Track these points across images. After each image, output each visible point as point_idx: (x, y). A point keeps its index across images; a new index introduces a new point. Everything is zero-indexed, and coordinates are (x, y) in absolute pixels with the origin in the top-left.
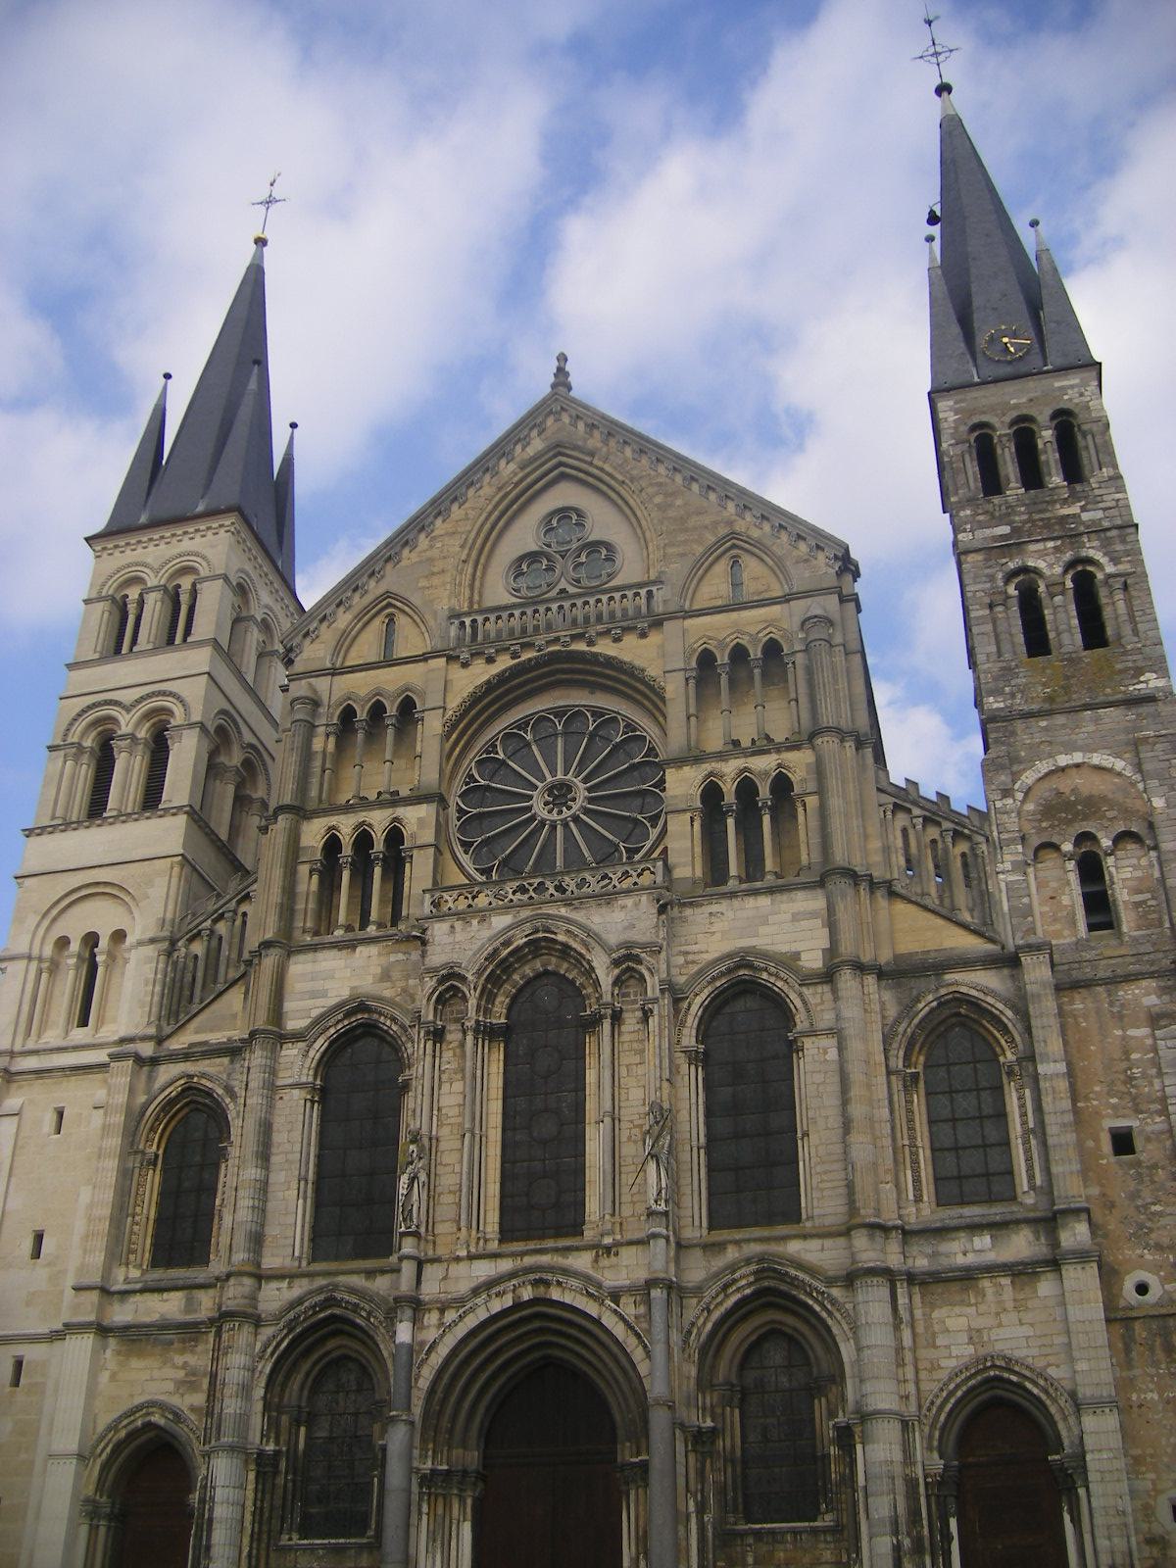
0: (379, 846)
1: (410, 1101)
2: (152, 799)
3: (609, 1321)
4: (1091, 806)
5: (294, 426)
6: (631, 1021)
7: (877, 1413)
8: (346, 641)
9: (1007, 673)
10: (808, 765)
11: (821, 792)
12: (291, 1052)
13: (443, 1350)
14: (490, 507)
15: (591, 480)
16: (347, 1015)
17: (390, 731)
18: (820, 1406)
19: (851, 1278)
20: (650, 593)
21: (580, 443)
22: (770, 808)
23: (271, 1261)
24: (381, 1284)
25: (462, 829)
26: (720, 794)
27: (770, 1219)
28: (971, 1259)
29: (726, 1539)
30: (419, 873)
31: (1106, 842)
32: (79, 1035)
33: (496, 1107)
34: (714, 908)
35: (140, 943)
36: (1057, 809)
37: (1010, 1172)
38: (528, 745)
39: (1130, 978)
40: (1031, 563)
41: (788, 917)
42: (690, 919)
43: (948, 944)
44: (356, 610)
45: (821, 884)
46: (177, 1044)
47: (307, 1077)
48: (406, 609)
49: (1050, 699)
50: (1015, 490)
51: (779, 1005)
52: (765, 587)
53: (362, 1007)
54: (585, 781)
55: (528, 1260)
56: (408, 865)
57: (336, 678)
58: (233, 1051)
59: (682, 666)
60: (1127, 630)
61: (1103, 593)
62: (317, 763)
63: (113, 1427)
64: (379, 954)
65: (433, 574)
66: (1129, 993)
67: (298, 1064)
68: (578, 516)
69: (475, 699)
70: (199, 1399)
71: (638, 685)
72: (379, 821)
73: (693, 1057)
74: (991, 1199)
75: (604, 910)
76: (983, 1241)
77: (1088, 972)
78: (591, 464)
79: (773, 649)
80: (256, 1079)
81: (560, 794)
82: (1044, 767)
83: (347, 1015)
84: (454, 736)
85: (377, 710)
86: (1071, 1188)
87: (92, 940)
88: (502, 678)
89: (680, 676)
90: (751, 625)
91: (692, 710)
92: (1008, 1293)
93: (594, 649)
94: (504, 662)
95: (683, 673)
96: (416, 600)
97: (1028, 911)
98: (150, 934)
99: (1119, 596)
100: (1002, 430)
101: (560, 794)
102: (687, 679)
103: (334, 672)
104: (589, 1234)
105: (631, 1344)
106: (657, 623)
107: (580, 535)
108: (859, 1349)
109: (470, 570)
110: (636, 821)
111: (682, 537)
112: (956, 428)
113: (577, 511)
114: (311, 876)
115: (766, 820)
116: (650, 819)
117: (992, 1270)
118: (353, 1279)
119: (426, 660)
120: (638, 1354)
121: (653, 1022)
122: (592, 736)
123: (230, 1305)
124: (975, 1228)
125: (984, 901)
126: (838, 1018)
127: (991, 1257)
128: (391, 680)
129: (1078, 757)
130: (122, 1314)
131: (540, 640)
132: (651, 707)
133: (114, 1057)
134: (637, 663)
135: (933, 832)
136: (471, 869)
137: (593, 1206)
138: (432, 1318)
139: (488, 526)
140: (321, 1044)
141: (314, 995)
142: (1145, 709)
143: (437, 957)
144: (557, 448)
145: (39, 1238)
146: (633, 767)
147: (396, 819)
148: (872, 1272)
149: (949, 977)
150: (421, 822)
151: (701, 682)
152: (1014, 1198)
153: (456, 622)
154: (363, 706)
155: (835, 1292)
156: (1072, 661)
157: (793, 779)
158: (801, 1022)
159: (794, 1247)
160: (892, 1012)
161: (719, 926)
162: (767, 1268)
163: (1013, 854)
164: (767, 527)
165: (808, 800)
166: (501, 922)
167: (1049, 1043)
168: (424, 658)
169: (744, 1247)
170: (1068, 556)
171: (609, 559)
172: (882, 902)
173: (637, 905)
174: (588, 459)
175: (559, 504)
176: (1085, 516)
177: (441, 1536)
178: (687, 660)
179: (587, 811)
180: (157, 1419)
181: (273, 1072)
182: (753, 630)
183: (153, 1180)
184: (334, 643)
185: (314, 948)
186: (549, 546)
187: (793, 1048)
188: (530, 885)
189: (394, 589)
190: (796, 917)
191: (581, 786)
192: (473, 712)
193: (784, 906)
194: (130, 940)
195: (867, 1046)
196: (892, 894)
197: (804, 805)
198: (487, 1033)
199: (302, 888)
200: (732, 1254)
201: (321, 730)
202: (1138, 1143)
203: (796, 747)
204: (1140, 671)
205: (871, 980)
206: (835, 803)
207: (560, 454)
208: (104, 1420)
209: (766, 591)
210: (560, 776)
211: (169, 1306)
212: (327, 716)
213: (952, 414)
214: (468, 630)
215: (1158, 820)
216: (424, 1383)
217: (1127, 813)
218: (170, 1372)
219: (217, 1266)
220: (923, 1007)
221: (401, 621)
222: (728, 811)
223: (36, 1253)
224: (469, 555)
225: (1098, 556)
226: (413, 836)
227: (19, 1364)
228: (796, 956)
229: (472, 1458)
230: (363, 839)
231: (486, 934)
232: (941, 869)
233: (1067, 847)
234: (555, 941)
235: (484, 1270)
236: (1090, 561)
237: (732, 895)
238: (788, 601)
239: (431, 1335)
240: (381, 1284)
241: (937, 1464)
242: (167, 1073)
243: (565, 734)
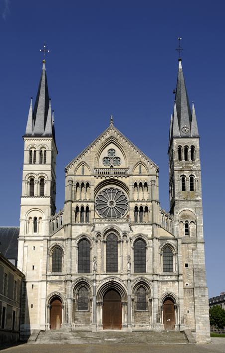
1: (92, 251)
2: (42, 194)
3: (122, 284)
4: (188, 216)
6: (125, 242)
7: (155, 298)
8: (76, 169)
9: (179, 193)
11: (152, 210)
12: (73, 241)
13: (100, 287)
16: (82, 236)
18: (147, 297)
19: (153, 281)
23: (73, 273)
24: (89, 277)
26: (137, 208)
27: (142, 272)
28: (167, 279)
29: (135, 312)
30: (91, 214)
31: (189, 222)
32: (35, 234)
33: (105, 253)
35: (45, 220)
36: (184, 216)
37: (173, 268)
39: (190, 243)
40: (185, 174)
43: (167, 235)
45: (152, 225)
46: (53, 237)
47: (76, 245)
49: (185, 198)
50: (184, 160)
51: (145, 242)
53: (84, 236)
55: (111, 275)
58: (63, 240)
60: (197, 189)
61: (194, 181)
62: (73, 193)
63: (50, 295)
66: (190, 245)
67: (75, 243)
69: (99, 185)
70: (64, 292)
72: (85, 205)
73: (133, 249)
74: (170, 272)
76: (169, 277)
77: (185, 242)
79: (146, 184)
80: (69, 245)
81: (112, 203)
82: (183, 209)
83: (82, 236)
85: (83, 184)
86: (181, 272)
87: (35, 219)
88: (104, 181)
90: (143, 179)
92: (171, 284)
93: (118, 179)
94: (104, 179)
97: (178, 232)
98: (46, 219)
99: (197, 182)
100: (183, 148)
101: (112, 203)
104: (119, 272)
105: (125, 287)
106: (128, 176)
108: (153, 290)
111: (132, 160)
117: (170, 281)
118: (85, 276)
120: (126, 289)
121: (128, 243)
123: (68, 279)
124: (168, 275)
125: (173, 229)
126: (153, 245)
127: (170, 279)
128: (85, 179)
129: (187, 209)
130: (49, 279)
133: (44, 239)
137: (119, 268)
138: (98, 282)
140: (78, 240)
141: (76, 232)
142: (198, 202)
143: (97, 229)
144: (112, 137)
145: (33, 267)
148: (156, 280)
149: (168, 241)
150: (92, 206)
152: (172, 272)
155: (151, 282)
156: (188, 193)
158: (148, 245)
159: (145, 276)
160: (160, 245)
161: (137, 229)
162: (142, 278)
163: (177, 223)
166: (106, 225)
167: (180, 252)
169: (139, 276)
170: (190, 174)
176: (194, 167)
177: (99, 311)
180: (56, 294)
181: (71, 244)
182: (143, 180)
183: (51, 258)
185: (76, 225)
187: (146, 248)
190: (148, 229)
194: (43, 219)
195: (158, 251)
198: (104, 242)
199: (73, 215)
200: (137, 276)
201: (73, 186)
202: (189, 266)
203: (149, 202)
204: (198, 196)
205: (158, 240)
206: (154, 212)
208: (48, 294)
211: (57, 278)
212: (75, 184)
215: (197, 221)
216: (97, 291)
217: (193, 218)
218: (57, 287)
219: (64, 272)
220: (164, 245)
223: (33, 269)
225: (194, 175)
227: (33, 285)
228: (147, 235)
229: (102, 301)
230: (82, 208)
231: (104, 227)
232: (167, 225)
233: (184, 222)
235: (105, 276)
236: (193, 175)
237: (139, 225)
239: (98, 285)
240: (89, 277)
241: (162, 305)
242: (52, 242)
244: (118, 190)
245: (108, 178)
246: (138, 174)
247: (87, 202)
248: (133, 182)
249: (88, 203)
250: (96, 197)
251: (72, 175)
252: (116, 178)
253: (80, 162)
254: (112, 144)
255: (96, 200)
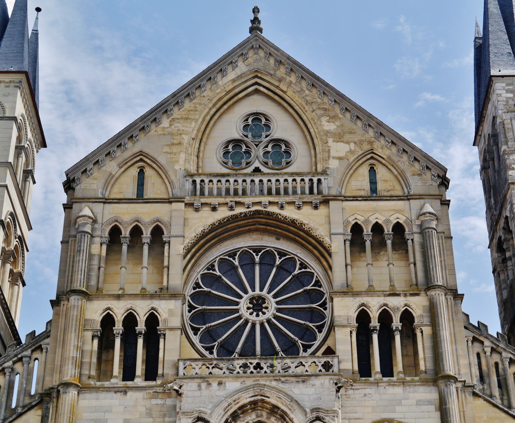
0: (141, 327)
5: (38, 10)
10: (424, 306)
11: (434, 323)
14: (211, 105)
15: (276, 98)
17: (146, 248)
20: (319, 181)
21: (272, 72)
22: (400, 331)
25: (192, 319)
34: (368, 391)
38: (235, 268)
41: (414, 402)
42: (352, 396)
44: (120, 160)
48: (154, 166)
52: (392, 187)
54: (275, 296)
56: (162, 341)
57: (107, 205)
59: (341, 231)
62: (95, 262)
64: (144, 399)
65: (173, 144)
68: (267, 120)
69: (204, 235)
71: (311, 239)
75: (301, 385)
78: (277, 87)
84: (189, 256)
85: (136, 232)
88: (222, 224)
89: (341, 238)
91: (349, 261)
94: (223, 213)
95: (342, 236)
96: (162, 159)
102: (345, 241)
103: (106, 201)
106: (326, 202)
107: (268, 133)
109: (197, 146)
110: (308, 328)
112: (507, 102)
113: (264, 115)
114: (93, 340)
115: (398, 338)
116: (317, 327)
119: (170, 202)
122: (279, 267)
131: (247, 200)
132: (318, 255)
134: (312, 225)
135: (496, 358)
136: (199, 346)
139: (208, 118)
144: (256, 74)
146: (305, 291)
147: (153, 309)
150: (171, 312)
151: (353, 243)
153: (191, 180)
154: (125, 228)
157: (414, 315)
164: (394, 149)
165: (423, 328)
166: (232, 385)
168: (169, 201)
171: (288, 153)
172: (470, 398)
173: (322, 384)
174: (277, 84)
175: (254, 110)
178: (345, 227)
179: (276, 317)
184: (103, 181)
185: (97, 389)
186: (247, 136)
188: (251, 363)
189: (146, 150)
191: (273, 301)
192: (202, 242)
193: (411, 395)
196: (475, 394)
197: (422, 332)
199: (87, 347)
201: (97, 240)
207: (256, 77)
209: (392, 190)
210: (257, 291)
213: (504, 92)
214: (198, 187)
221: (148, 172)
222: (374, 330)
224: (197, 135)
226: (165, 321)
234: (268, 403)
238: (409, 199)
243: (260, 264)
244: (282, 254)
245: (239, 210)
246: (362, 193)
247: (152, 296)
248: (346, 223)
249: (156, 303)
250: (191, 284)
251: (96, 200)
252: (274, 209)
253: (128, 154)
254: (256, 98)
255: (189, 291)
